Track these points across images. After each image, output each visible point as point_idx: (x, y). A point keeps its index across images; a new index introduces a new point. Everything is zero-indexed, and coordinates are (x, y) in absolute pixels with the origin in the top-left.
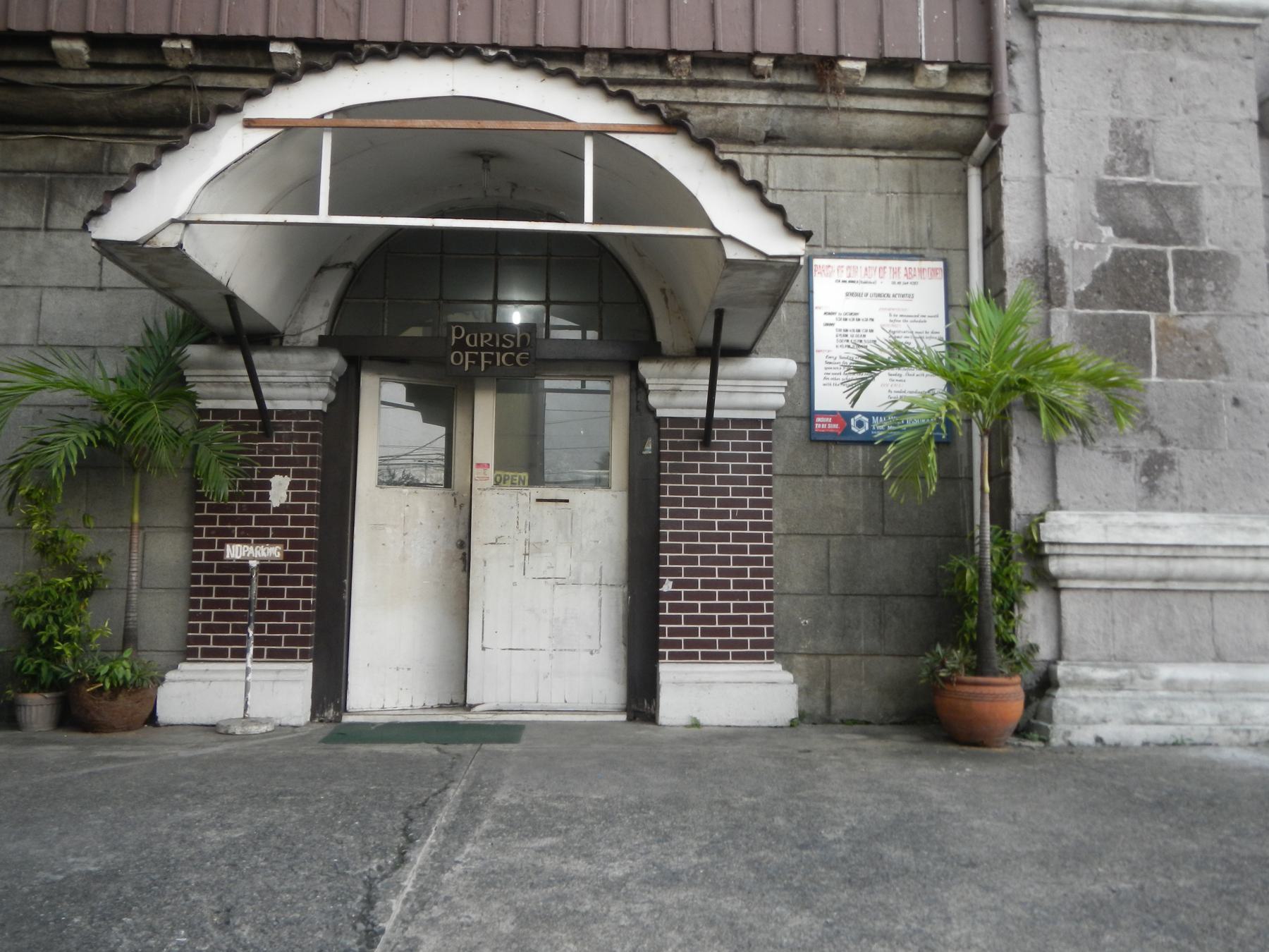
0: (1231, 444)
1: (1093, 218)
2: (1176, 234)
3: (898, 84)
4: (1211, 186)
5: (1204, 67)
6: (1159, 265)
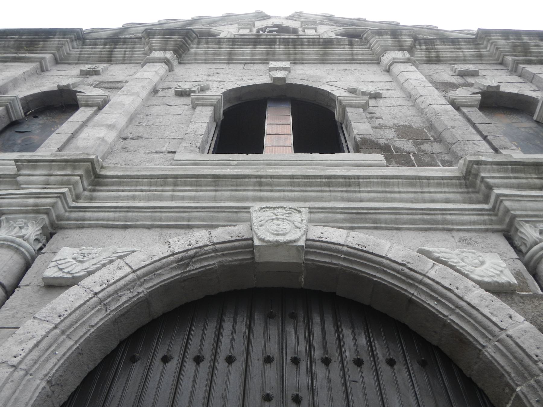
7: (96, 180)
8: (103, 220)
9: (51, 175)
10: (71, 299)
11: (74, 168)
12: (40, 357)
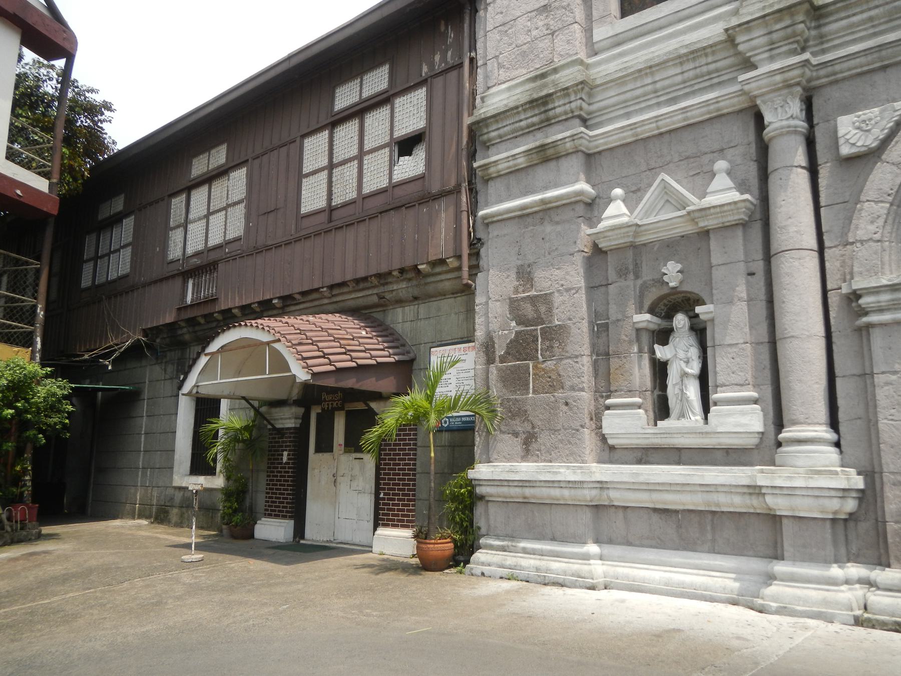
0: (563, 426)
1: (508, 318)
2: (542, 319)
3: (444, 268)
4: (559, 291)
5: (559, 228)
6: (534, 336)
7: (818, 13)
8: (856, 68)
9: (770, 33)
10: (890, 178)
11: (792, 15)
12: (892, 229)
